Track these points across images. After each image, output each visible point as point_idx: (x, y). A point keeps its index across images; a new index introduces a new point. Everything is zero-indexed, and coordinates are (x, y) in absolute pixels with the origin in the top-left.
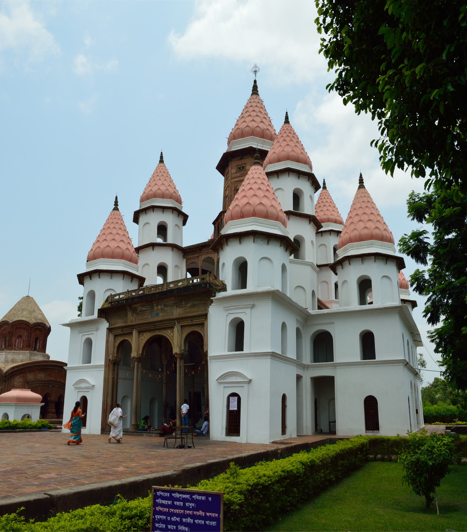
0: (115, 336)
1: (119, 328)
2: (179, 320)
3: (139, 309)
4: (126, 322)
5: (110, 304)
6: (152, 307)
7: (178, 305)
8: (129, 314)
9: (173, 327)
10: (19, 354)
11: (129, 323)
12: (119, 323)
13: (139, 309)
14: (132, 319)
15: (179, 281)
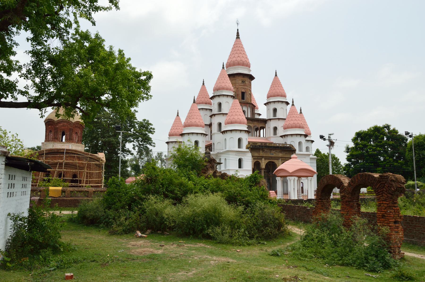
0: (254, 159)
1: (256, 156)
2: (281, 158)
3: (266, 150)
4: (259, 154)
5: (251, 146)
6: (271, 151)
7: (281, 152)
8: (261, 151)
9: (278, 160)
10: (79, 147)
11: (261, 155)
12: (256, 154)
13: (266, 150)
14: (261, 154)
15: (281, 144)
